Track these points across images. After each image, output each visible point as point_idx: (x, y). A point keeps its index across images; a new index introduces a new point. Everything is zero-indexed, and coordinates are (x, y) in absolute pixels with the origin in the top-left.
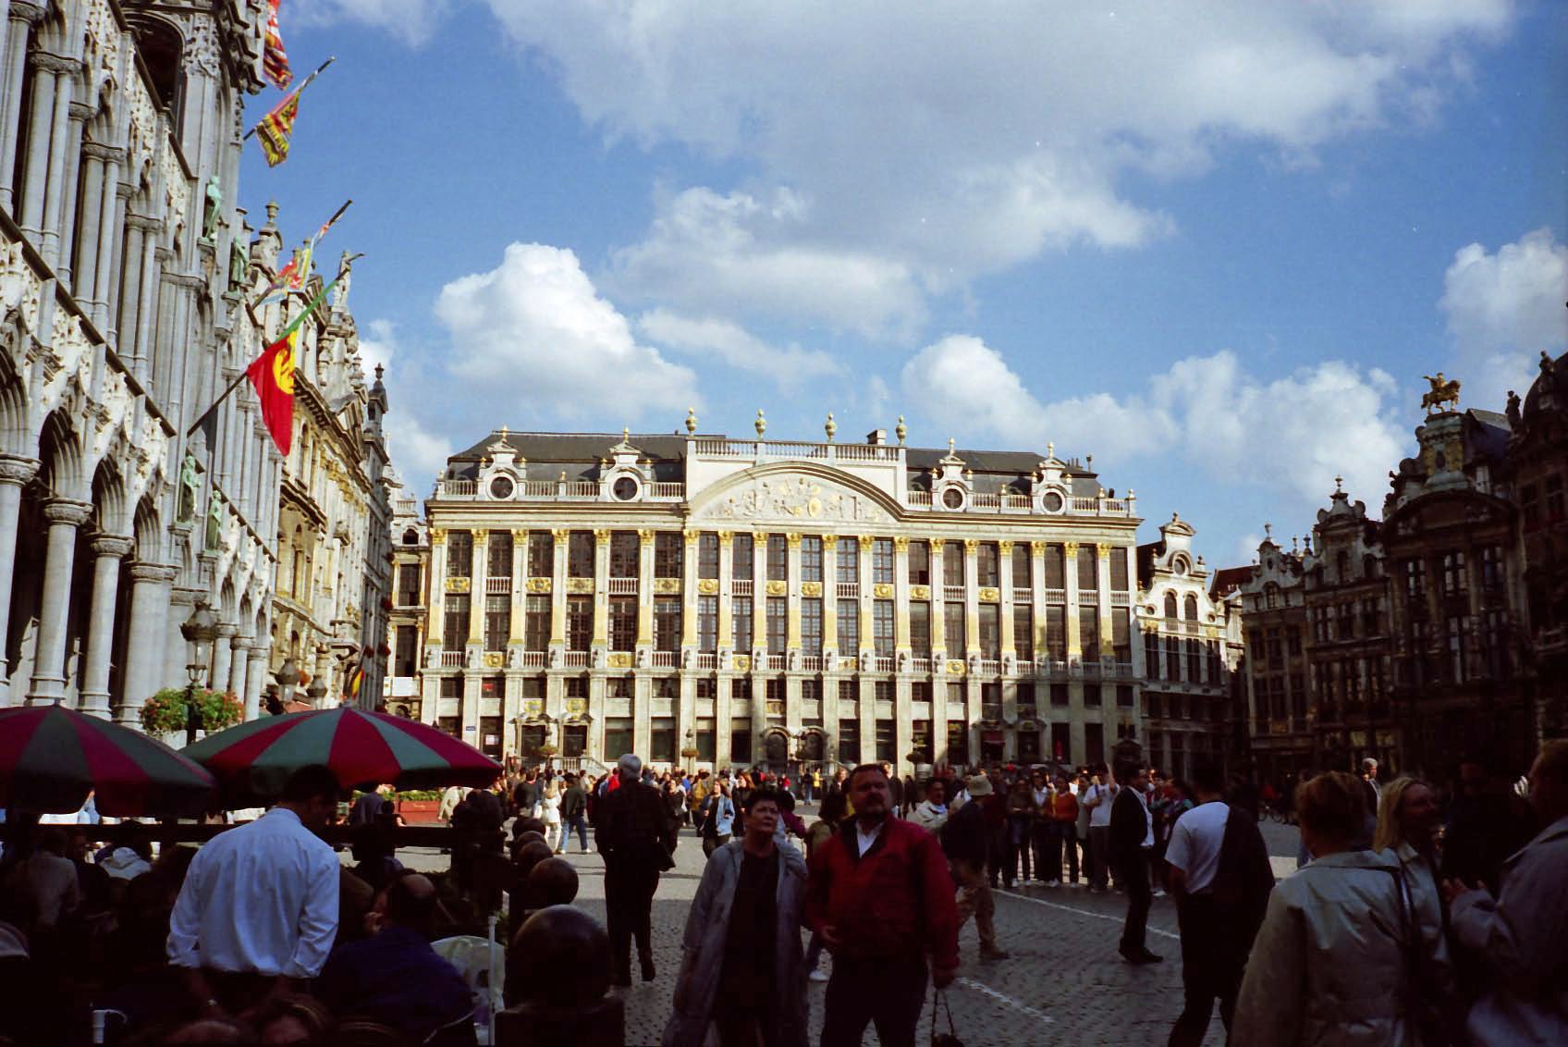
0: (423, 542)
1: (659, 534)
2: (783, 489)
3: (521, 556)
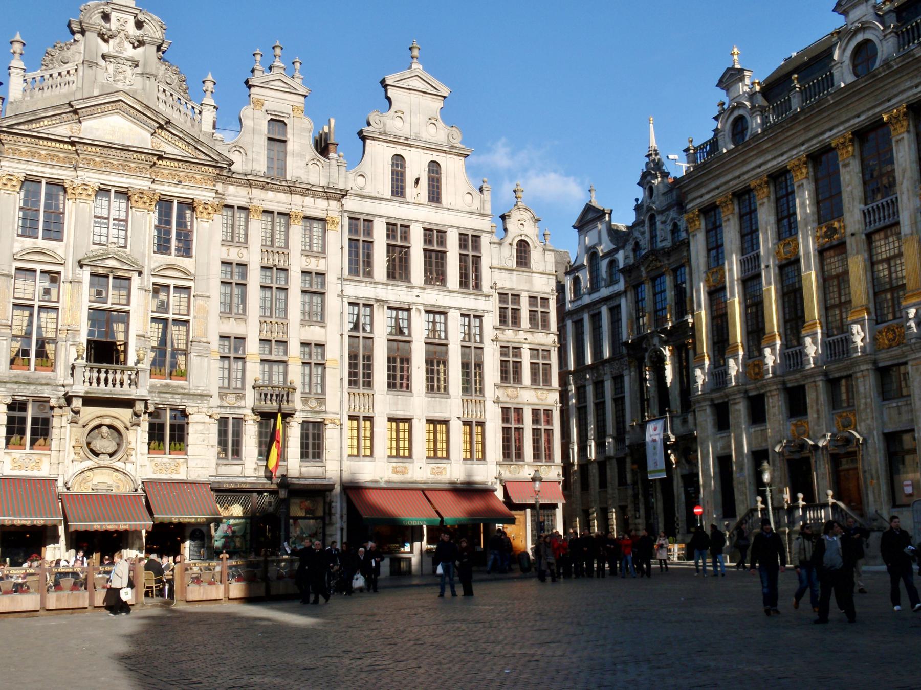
0: (683, 235)
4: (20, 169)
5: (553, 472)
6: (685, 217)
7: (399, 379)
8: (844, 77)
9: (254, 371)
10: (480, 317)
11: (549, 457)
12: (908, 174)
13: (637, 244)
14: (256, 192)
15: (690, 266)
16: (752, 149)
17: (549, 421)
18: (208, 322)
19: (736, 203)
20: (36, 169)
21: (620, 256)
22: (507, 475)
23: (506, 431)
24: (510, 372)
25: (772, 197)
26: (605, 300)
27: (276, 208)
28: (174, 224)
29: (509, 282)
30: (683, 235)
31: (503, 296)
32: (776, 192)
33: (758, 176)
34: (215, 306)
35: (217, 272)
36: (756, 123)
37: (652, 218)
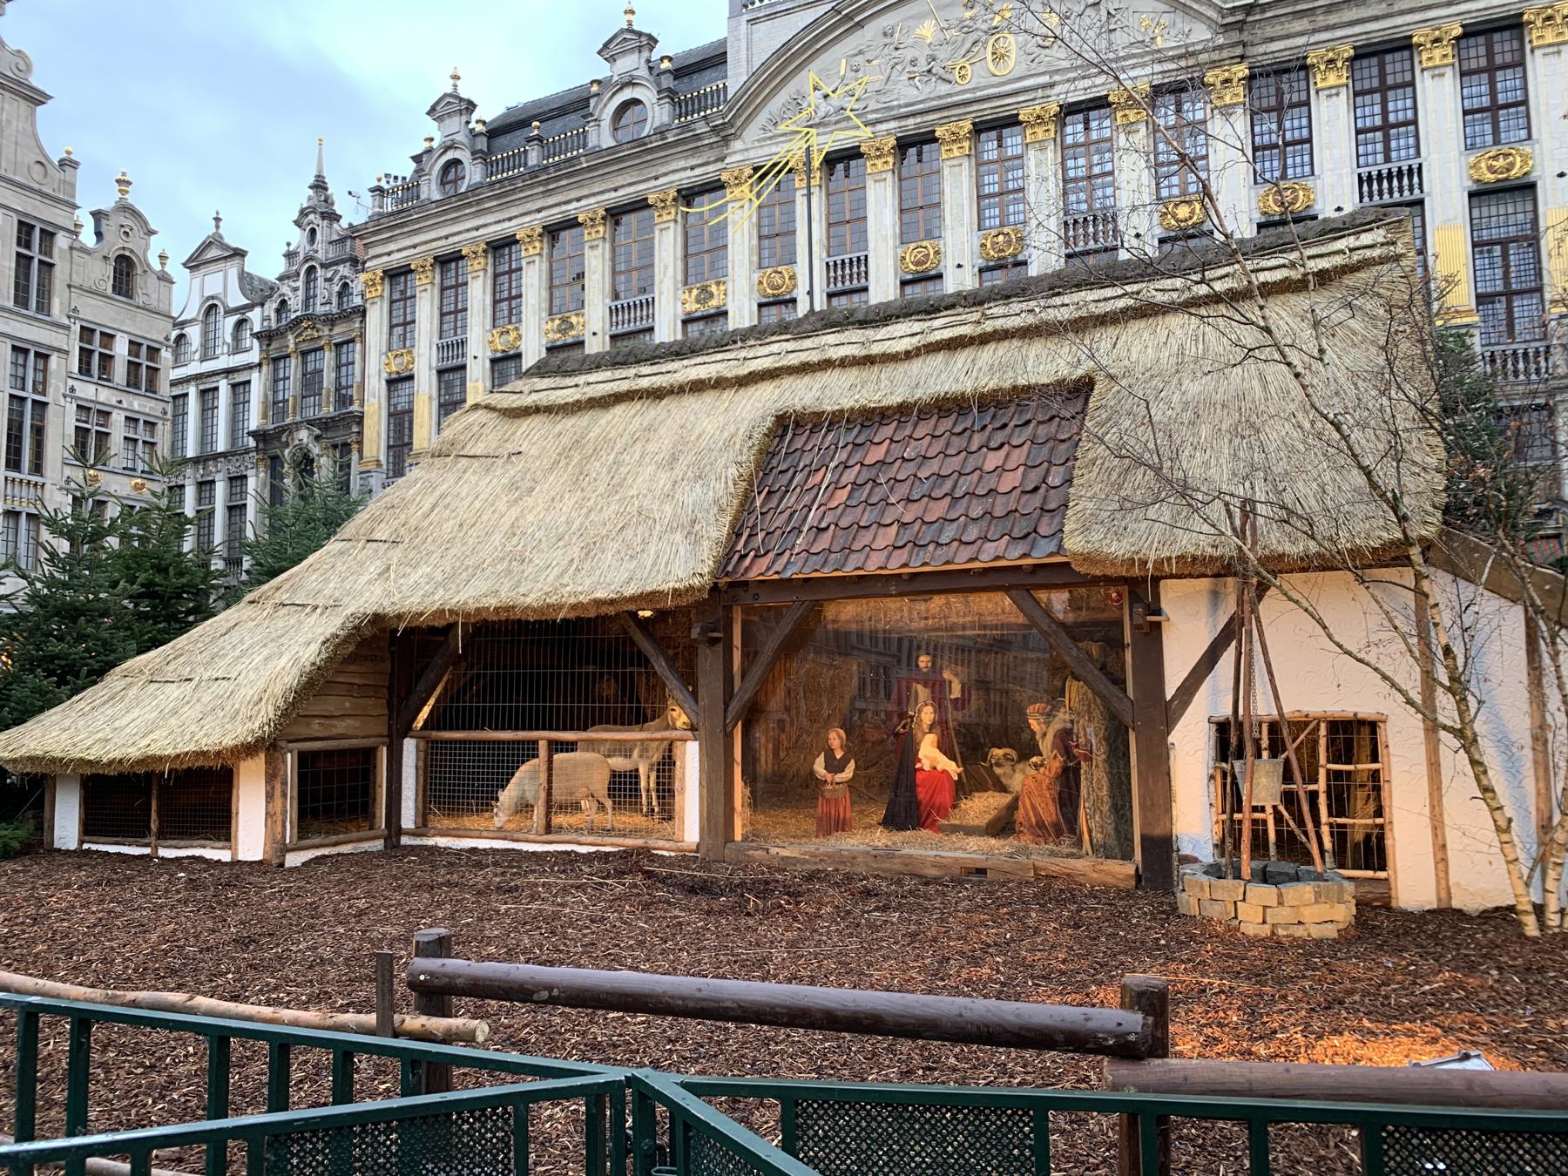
1: (688, 196)
2: (928, 30)
3: (478, 293)
6: (363, 277)
8: (602, 136)
10: (46, 357)
12: (670, 272)
13: (283, 302)
15: (363, 342)
16: (470, 205)
19: (438, 270)
21: (255, 316)
25: (490, 270)
26: (228, 372)
29: (102, 313)
30: (358, 301)
31: (87, 333)
32: (495, 266)
33: (474, 241)
36: (473, 173)
37: (311, 269)
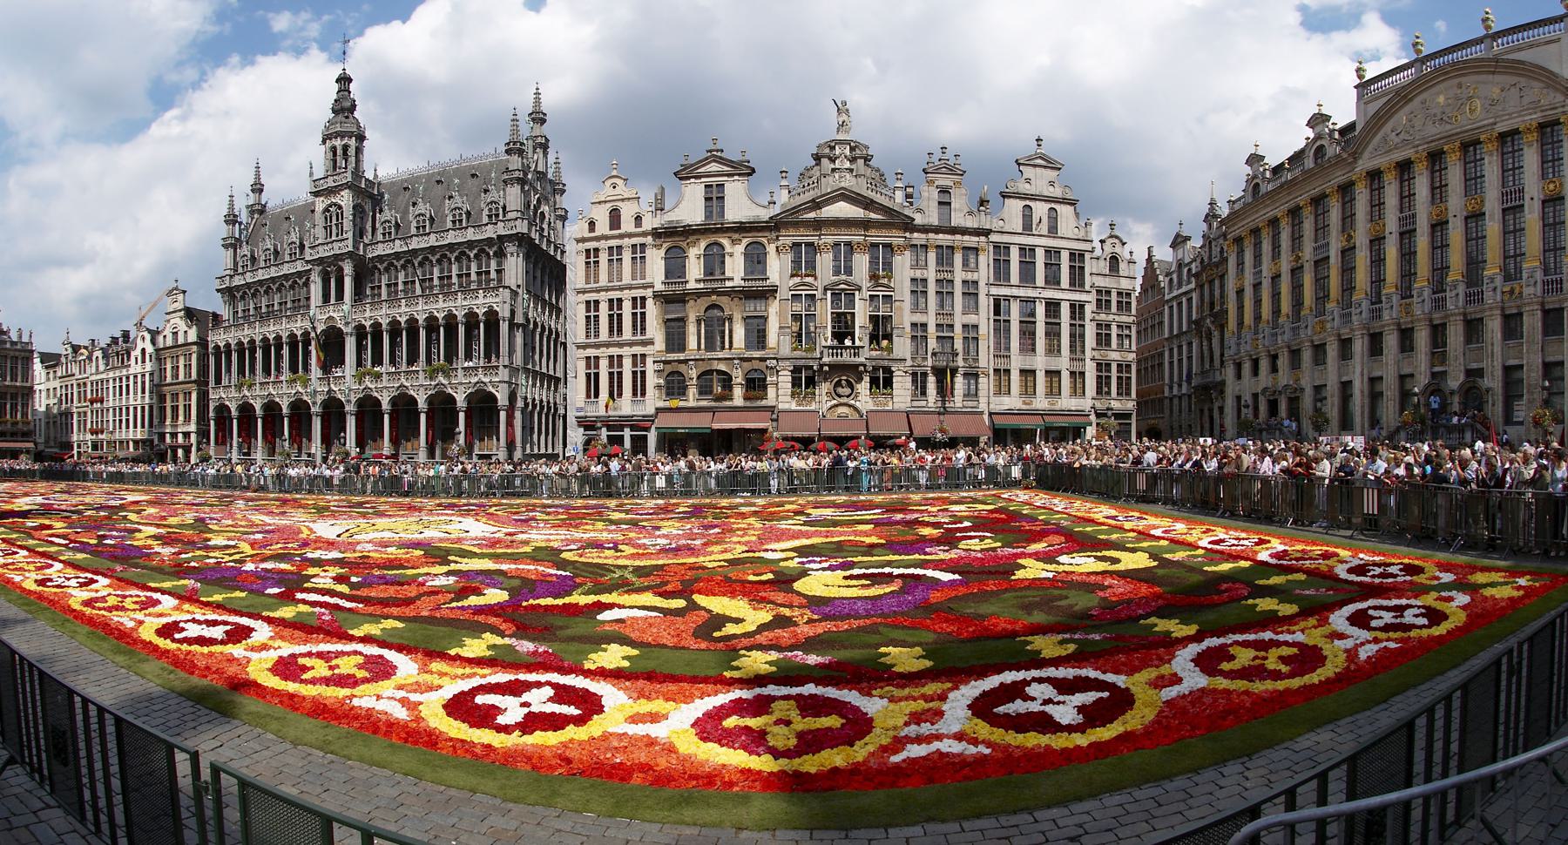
4: (788, 241)
5: (1130, 405)
7: (1029, 346)
9: (932, 344)
11: (1128, 394)
14: (931, 235)
17: (1129, 371)
18: (904, 317)
20: (798, 239)
22: (1098, 405)
23: (1099, 377)
24: (1103, 340)
27: (945, 244)
28: (883, 257)
34: (907, 305)
35: (907, 286)
